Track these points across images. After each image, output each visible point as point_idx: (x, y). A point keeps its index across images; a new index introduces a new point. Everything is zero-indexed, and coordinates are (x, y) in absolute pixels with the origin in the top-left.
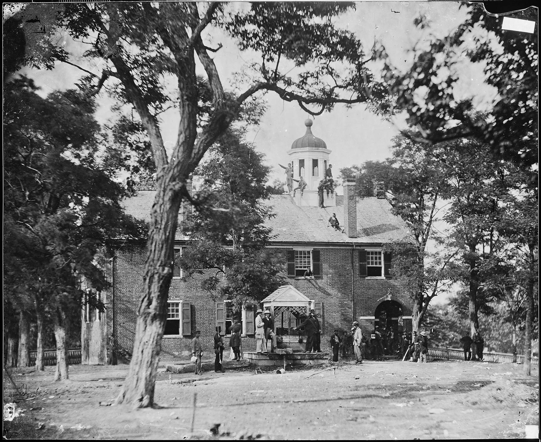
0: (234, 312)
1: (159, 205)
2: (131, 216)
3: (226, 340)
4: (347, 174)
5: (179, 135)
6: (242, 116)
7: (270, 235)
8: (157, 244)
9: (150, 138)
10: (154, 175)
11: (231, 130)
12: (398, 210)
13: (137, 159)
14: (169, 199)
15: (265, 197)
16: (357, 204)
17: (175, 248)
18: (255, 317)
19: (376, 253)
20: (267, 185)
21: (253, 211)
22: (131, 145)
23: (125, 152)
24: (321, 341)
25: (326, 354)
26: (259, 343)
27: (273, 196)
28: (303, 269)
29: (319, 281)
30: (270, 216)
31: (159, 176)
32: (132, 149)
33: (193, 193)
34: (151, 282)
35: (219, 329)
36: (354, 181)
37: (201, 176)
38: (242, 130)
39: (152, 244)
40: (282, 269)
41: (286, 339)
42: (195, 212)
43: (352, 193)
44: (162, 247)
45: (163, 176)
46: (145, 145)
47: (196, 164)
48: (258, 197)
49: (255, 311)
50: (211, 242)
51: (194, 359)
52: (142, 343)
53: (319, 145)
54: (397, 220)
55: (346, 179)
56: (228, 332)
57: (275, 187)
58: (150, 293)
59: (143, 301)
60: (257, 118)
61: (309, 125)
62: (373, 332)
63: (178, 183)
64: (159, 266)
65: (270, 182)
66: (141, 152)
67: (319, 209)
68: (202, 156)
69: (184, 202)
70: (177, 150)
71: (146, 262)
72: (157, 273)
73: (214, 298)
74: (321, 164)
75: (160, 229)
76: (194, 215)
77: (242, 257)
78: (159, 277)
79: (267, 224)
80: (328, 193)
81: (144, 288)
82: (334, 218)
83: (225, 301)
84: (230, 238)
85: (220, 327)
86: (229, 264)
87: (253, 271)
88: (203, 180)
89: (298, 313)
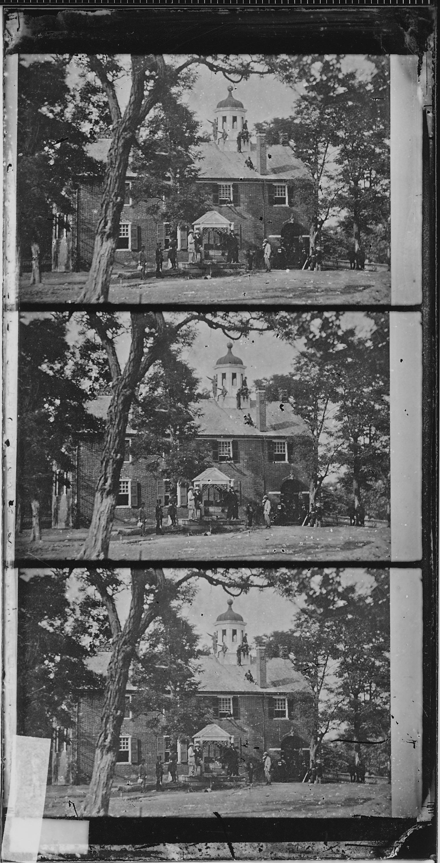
19: (281, 187)
21: (187, 155)
22: (93, 104)
26: (191, 256)
33: (141, 140)
47: (143, 118)
49: (188, 231)
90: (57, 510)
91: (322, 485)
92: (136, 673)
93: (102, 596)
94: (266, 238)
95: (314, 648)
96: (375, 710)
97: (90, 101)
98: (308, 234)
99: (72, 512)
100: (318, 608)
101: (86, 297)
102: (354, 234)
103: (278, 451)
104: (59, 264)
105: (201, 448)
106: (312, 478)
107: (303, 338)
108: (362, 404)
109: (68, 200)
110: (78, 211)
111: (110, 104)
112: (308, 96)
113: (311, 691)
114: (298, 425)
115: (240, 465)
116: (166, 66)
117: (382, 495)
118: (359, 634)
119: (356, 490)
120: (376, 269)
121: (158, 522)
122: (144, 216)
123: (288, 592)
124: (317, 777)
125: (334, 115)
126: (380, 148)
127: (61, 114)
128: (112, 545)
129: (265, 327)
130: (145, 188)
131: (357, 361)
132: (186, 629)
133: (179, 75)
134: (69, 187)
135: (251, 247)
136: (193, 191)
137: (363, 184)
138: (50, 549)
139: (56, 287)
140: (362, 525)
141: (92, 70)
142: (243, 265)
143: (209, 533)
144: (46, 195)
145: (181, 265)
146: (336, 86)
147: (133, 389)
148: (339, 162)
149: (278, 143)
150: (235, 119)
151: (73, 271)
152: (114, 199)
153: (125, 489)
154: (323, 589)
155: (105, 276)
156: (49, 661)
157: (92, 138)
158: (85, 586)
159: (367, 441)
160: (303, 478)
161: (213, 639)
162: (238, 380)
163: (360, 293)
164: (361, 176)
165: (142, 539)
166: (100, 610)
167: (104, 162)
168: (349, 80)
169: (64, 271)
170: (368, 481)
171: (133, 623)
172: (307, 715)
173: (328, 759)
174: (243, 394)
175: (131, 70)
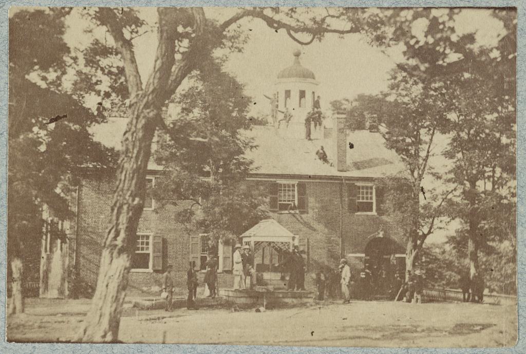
0: (210, 246)
1: (130, 133)
2: (99, 143)
3: (201, 276)
4: (337, 107)
5: (156, 61)
6: (225, 43)
7: (251, 167)
8: (128, 173)
9: (125, 62)
10: (127, 102)
11: (212, 57)
12: (392, 144)
13: (109, 84)
14: (142, 127)
15: (247, 127)
17: (147, 178)
18: (233, 251)
19: (367, 188)
20: (248, 116)
21: (234, 142)
22: (102, 69)
23: (96, 76)
24: (306, 279)
26: (237, 279)
27: (255, 126)
28: (287, 203)
29: (304, 216)
30: (252, 147)
31: (132, 103)
32: (104, 73)
33: (168, 122)
34: (119, 213)
36: (345, 114)
37: (177, 104)
38: (225, 58)
39: (121, 172)
40: (264, 202)
41: (267, 276)
42: (170, 141)
43: (342, 126)
44: (133, 177)
45: (136, 103)
46: (118, 70)
47: (173, 91)
48: (239, 128)
49: (233, 246)
50: (186, 173)
51: (164, 295)
52: (107, 277)
53: (308, 75)
54: (392, 154)
55: (336, 112)
56: (203, 267)
57: (258, 118)
58: (117, 224)
59: (109, 232)
60: (241, 46)
61: (297, 55)
62: (363, 270)
63: (153, 111)
64: (129, 196)
65: (252, 112)
66: (113, 77)
68: (179, 83)
69: (158, 130)
70: (153, 77)
71: (115, 192)
72: (125, 204)
73: (189, 231)
74: (308, 96)
75: (132, 157)
76: (168, 144)
77: (220, 189)
78: (128, 208)
79: (248, 155)
80: (316, 126)
81: (111, 220)
82: (321, 151)
83: (201, 235)
84: (207, 168)
85: (194, 262)
86: (206, 196)
87: (231, 204)
88: (180, 108)
89: (281, 249)
90: (47, 272)
91: (424, 246)
92: (162, 148)
93: (116, 40)
94: (343, 257)
95: (415, 118)
96: (499, 203)
97: (99, 66)
98: (404, 253)
99: (69, 276)
100: (422, 63)
101: (87, 333)
102: (469, 253)
103: (363, 198)
104: (50, 287)
105: (253, 192)
106: (410, 235)
107: (402, 44)
108: (483, 136)
109: (64, 201)
110: (78, 216)
112: (407, 64)
113: (410, 177)
114: (391, 163)
115: (309, 217)
116: (206, 20)
117: (509, 261)
118: (480, 99)
119: (472, 253)
120: (499, 302)
121: (191, 291)
122: (173, 225)
123: (380, 39)
124: (415, 294)
125: (444, 91)
126: (508, 137)
127: (57, 82)
128: (124, 321)
129: (348, 28)
130: (173, 187)
131: (478, 76)
132: (235, 88)
133: (224, 33)
134: (66, 183)
135: (321, 268)
136: (241, 192)
137: (483, 186)
138: (36, 325)
139: (46, 319)
140: (480, 301)
141: (103, 24)
142: (311, 293)
143: (262, 309)
144: (34, 192)
145: (222, 293)
146: (448, 51)
147: (159, 109)
148: (449, 155)
149: (364, 129)
150: (302, 94)
151: (70, 297)
152: (130, 201)
153: (145, 246)
154: (429, 37)
155: (114, 305)
156: (40, 128)
157: (100, 116)
158: (92, 26)
159: (489, 186)
160: (398, 235)
161: (272, 103)
162: (308, 100)
163: (476, 335)
164: (481, 174)
165: (167, 314)
166: (112, 60)
167: (116, 149)
168: (466, 44)
169: (56, 297)
170: (489, 240)
171: (160, 79)
172: (403, 209)
173: (431, 269)
174: (314, 119)
175: (158, 25)
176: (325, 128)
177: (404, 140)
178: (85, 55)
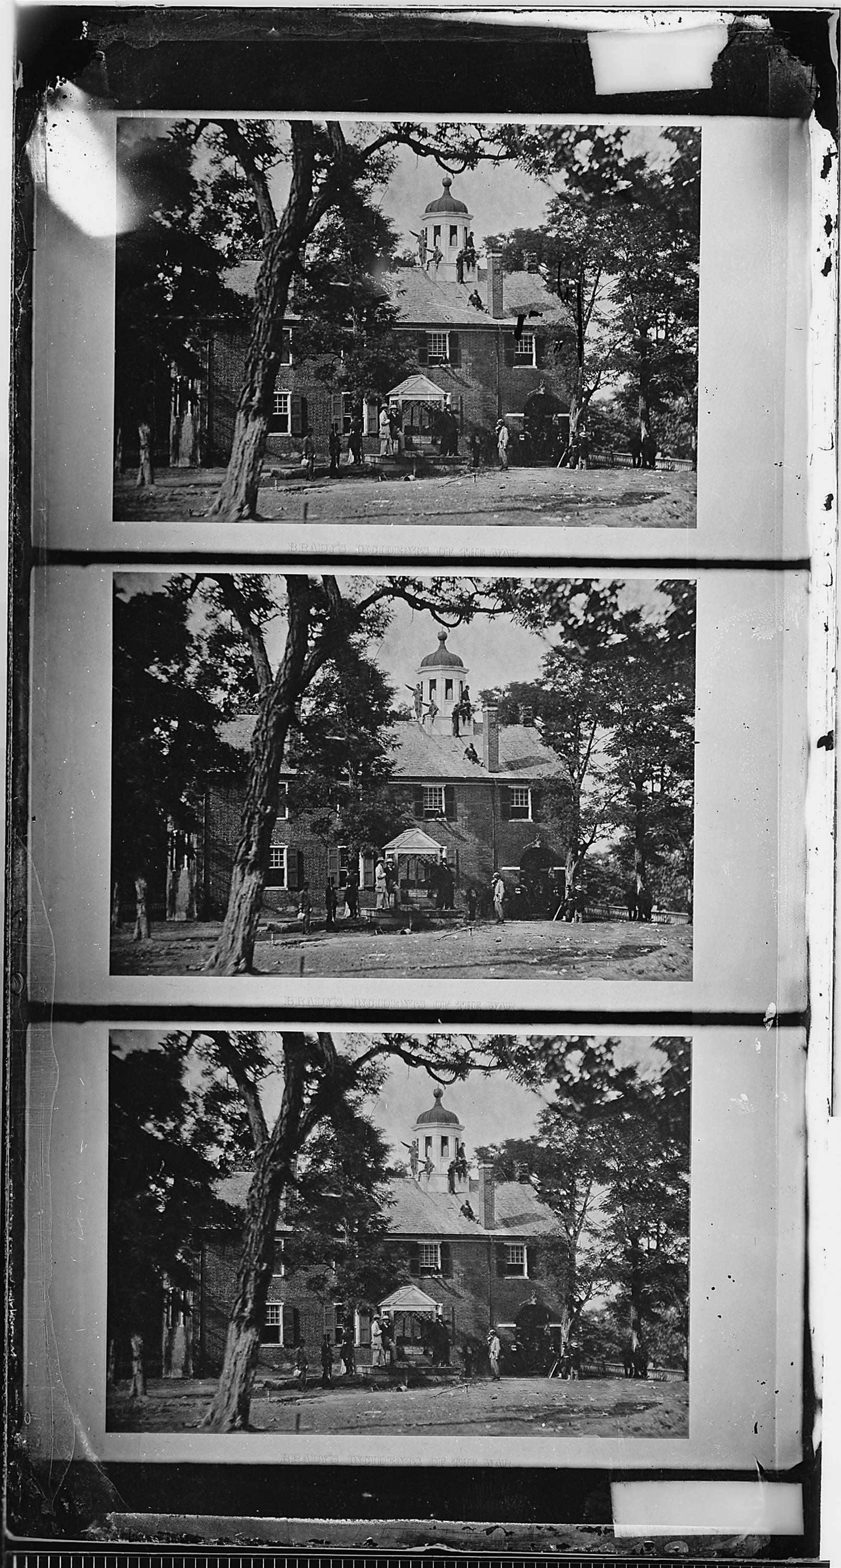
7: (390, 1225)
15: (384, 1180)
16: (496, 1190)
20: (386, 1166)
21: (370, 1197)
22: (224, 1117)
25: (457, 1369)
27: (393, 1179)
32: (226, 1122)
35: (327, 1337)
40: (404, 1266)
65: (390, 1163)
67: (449, 1195)
79: (386, 1212)
111: (251, 1117)
112: (561, 1104)
176: (470, 1179)
177: (558, 1193)
178: (204, 1101)
